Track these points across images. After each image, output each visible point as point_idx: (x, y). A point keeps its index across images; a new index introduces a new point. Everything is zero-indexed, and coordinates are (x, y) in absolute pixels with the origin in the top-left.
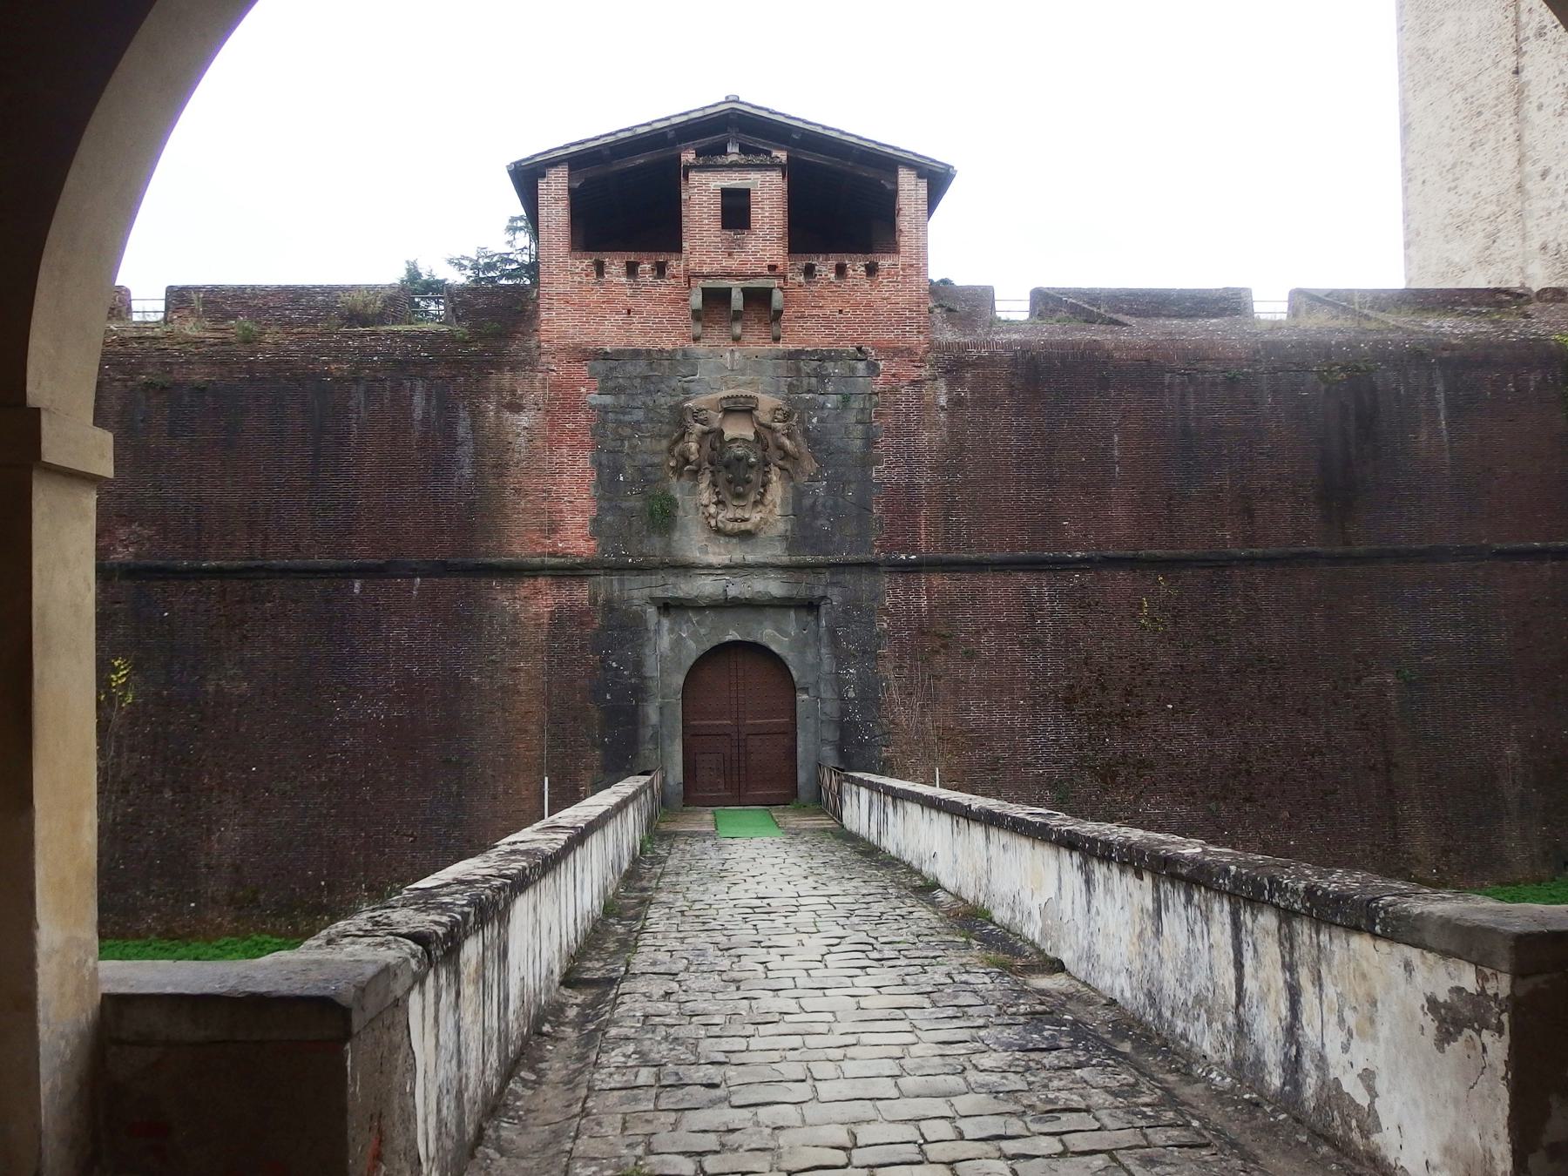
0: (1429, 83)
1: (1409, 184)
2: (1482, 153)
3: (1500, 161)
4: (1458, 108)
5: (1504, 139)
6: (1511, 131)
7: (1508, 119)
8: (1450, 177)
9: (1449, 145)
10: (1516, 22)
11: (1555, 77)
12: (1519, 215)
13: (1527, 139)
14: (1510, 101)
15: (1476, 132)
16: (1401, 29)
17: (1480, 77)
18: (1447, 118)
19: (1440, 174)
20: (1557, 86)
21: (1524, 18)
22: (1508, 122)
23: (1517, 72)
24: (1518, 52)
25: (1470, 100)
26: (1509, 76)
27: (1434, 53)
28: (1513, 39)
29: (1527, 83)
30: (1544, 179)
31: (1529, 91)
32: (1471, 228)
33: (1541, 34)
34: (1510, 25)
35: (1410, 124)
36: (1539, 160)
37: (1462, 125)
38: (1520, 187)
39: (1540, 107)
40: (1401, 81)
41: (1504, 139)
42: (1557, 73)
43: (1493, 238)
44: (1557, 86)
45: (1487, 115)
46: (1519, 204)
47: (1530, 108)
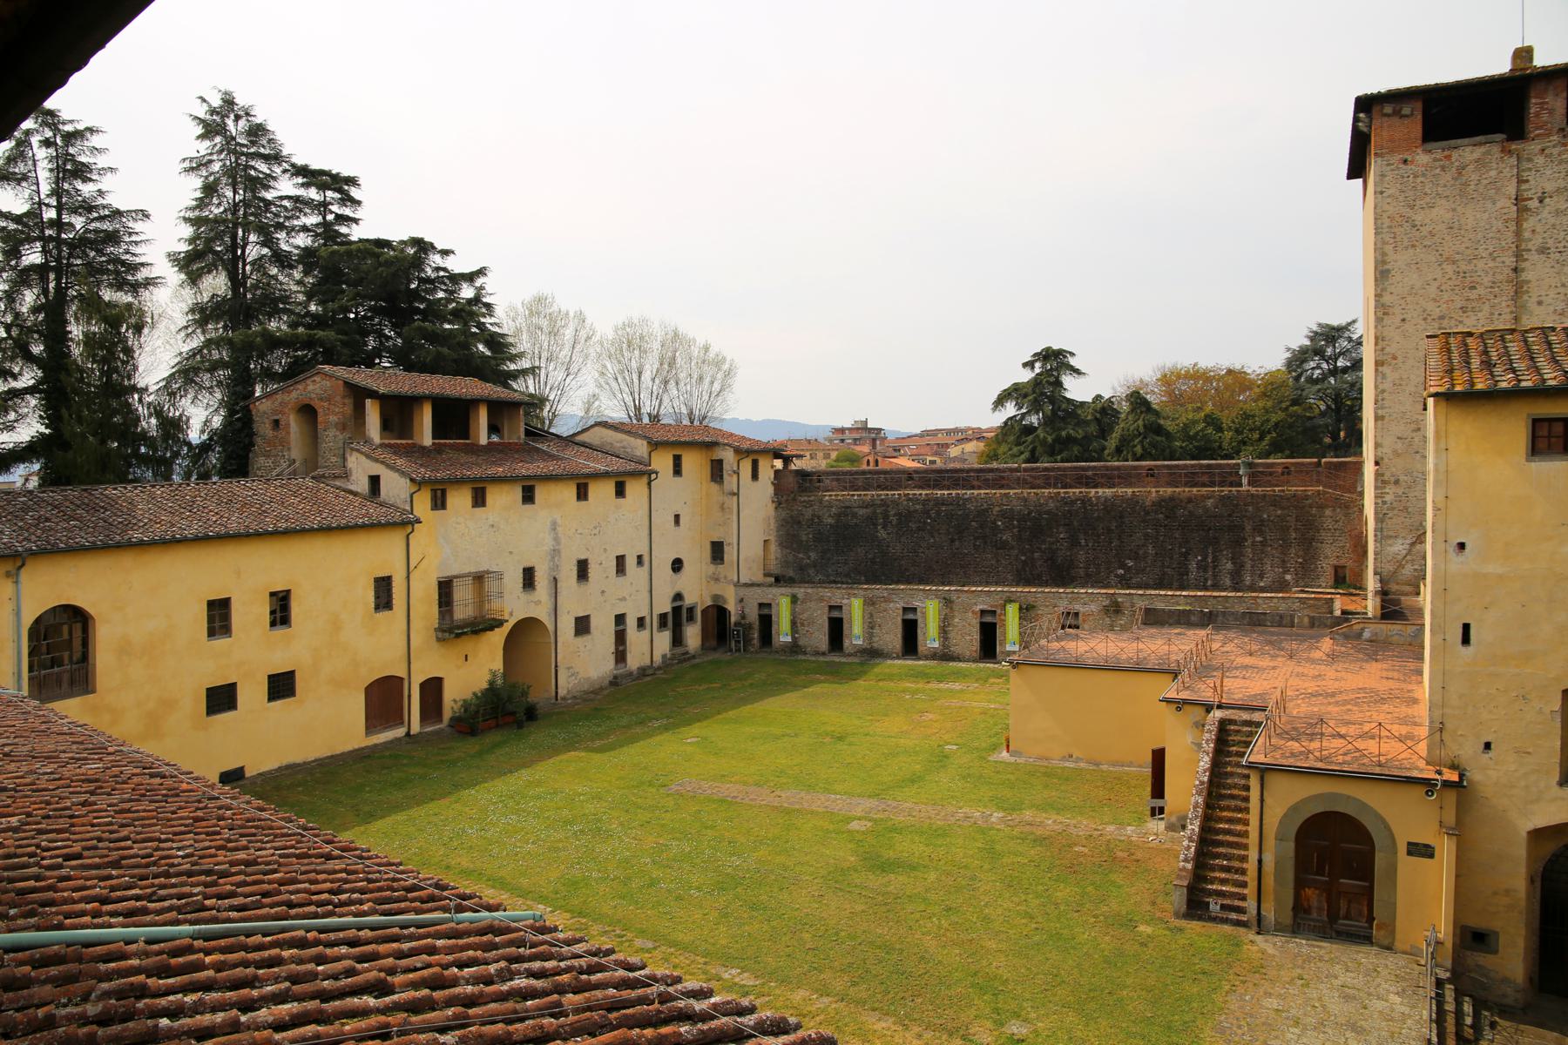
1: (1385, 317)
4: (1448, 277)
6: (1509, 310)
8: (1436, 325)
9: (1435, 300)
10: (1518, 233)
14: (1509, 290)
16: (1382, 193)
17: (1474, 261)
19: (1425, 319)
21: (1527, 235)
22: (1504, 304)
23: (1515, 270)
24: (1518, 256)
26: (1507, 271)
28: (1514, 246)
29: (1528, 282)
33: (1543, 250)
35: (1388, 271)
37: (1452, 290)
41: (1500, 314)
42: (1559, 285)
45: (1481, 291)
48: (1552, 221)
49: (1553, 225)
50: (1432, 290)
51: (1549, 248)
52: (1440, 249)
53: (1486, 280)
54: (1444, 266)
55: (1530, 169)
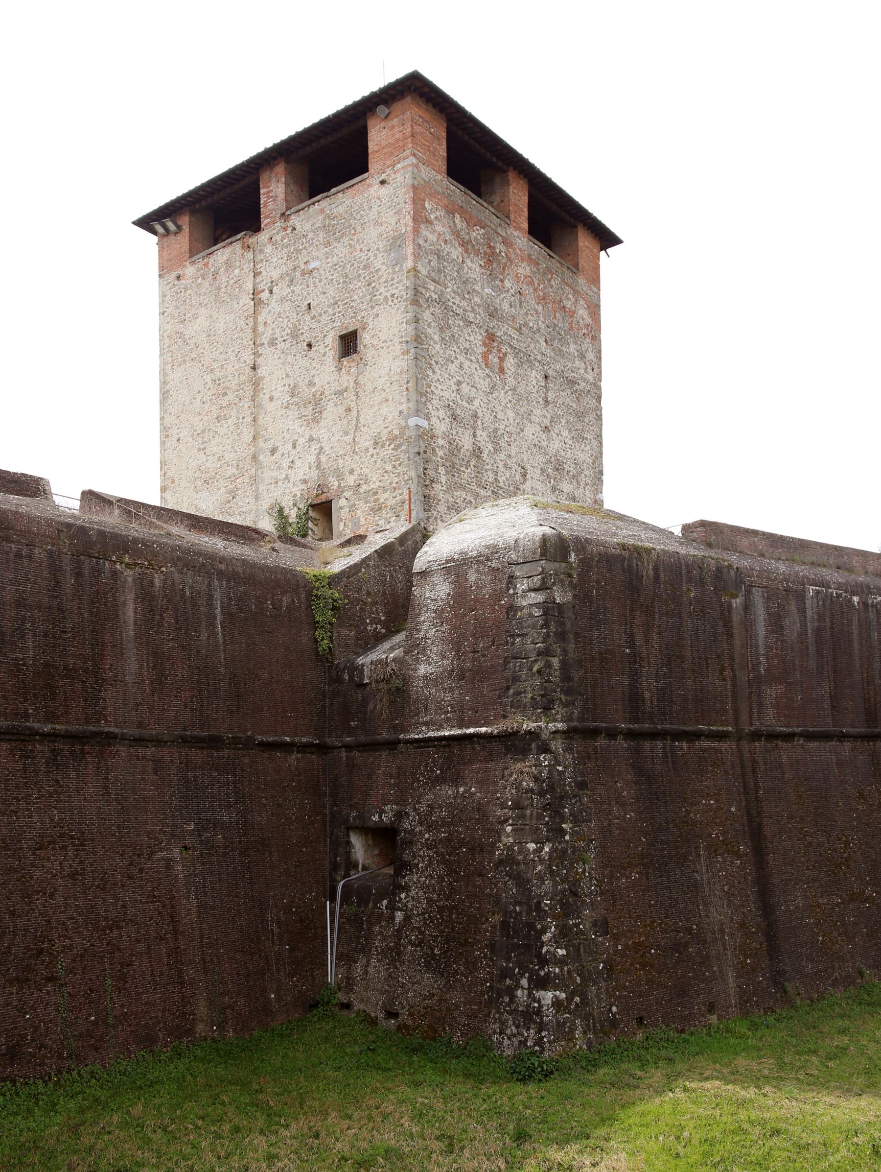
0: (185, 361)
2: (225, 426)
3: (239, 434)
5: (243, 418)
7: (247, 403)
11: (282, 378)
12: (254, 480)
13: (261, 421)
14: (249, 388)
15: (221, 408)
18: (199, 392)
20: (285, 385)
21: (261, 328)
22: (246, 407)
25: (217, 382)
26: (248, 370)
27: (190, 339)
29: (262, 378)
30: (273, 455)
31: (263, 384)
32: (216, 484)
33: (272, 343)
34: (249, 331)
36: (270, 439)
38: (255, 458)
39: (271, 399)
40: (162, 355)
41: (243, 418)
42: (284, 376)
43: (233, 494)
44: (285, 385)
45: (231, 396)
46: (253, 471)
47: (264, 398)
48: (278, 309)
49: (279, 314)
50: (198, 403)
51: (277, 339)
52: (202, 359)
53: (234, 383)
54: (205, 377)
55: (262, 261)
